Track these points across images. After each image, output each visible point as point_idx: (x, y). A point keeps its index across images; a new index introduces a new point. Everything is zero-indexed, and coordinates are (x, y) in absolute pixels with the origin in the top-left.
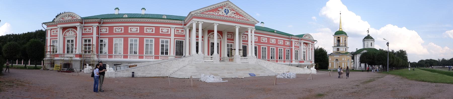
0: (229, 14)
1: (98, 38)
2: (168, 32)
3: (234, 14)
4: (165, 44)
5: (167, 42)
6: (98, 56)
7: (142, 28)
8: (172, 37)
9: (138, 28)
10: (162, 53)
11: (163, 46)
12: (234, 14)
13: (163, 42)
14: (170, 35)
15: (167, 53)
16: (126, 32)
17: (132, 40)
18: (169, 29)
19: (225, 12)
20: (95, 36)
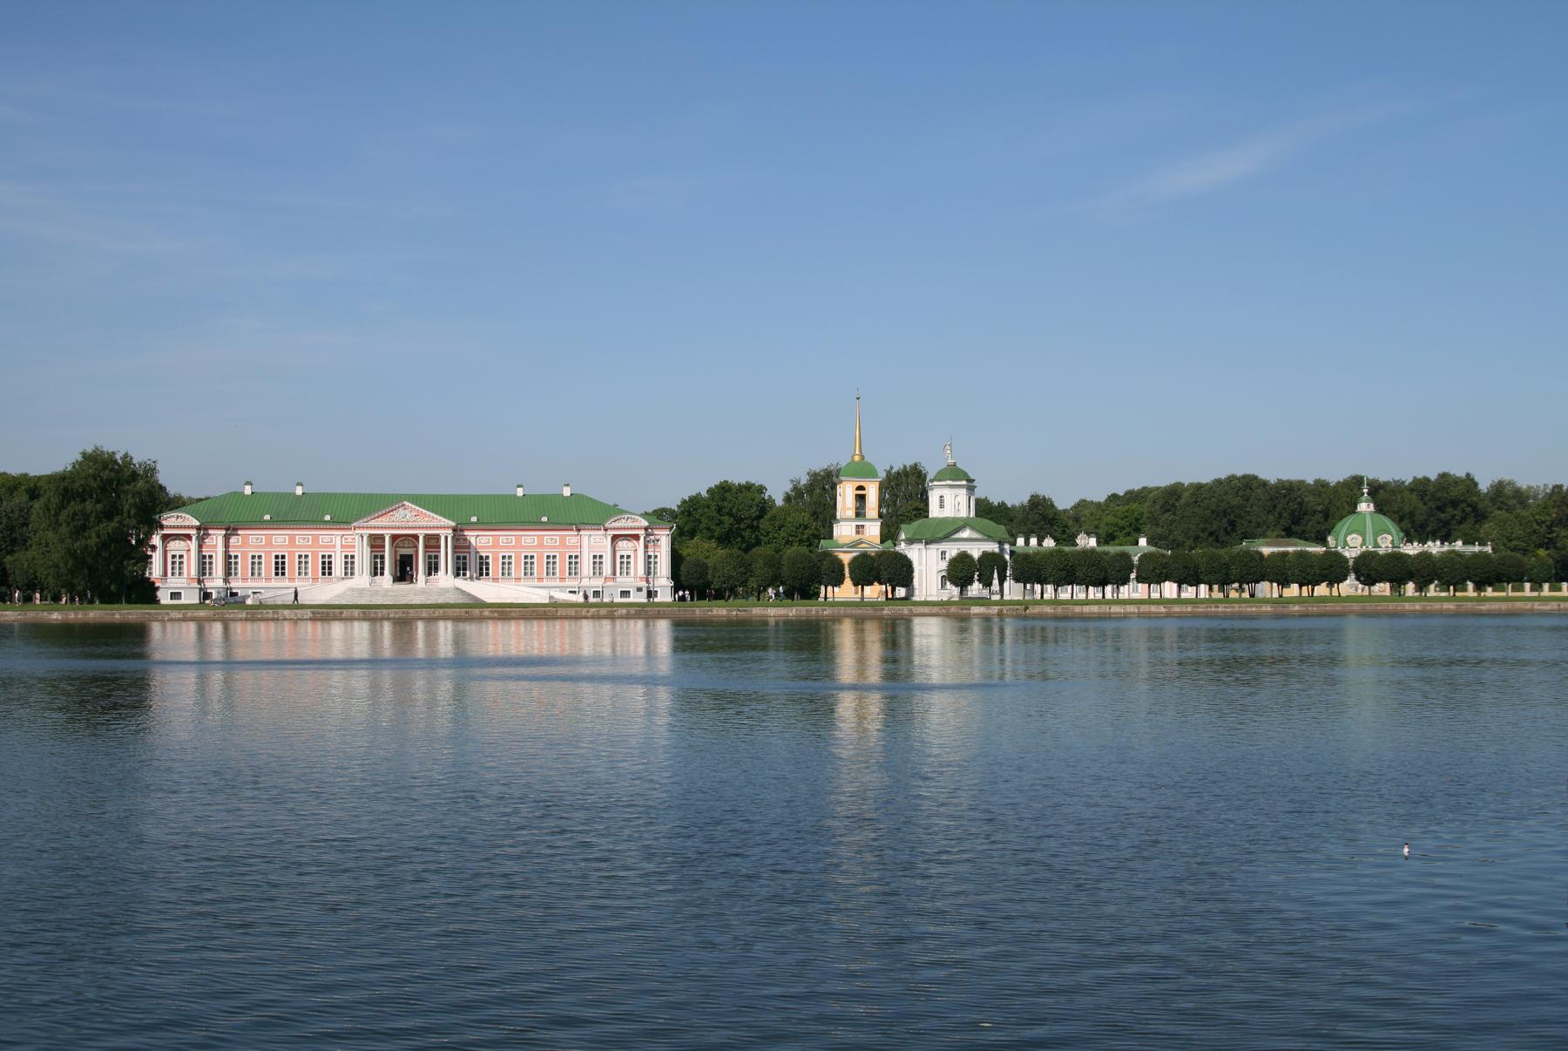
6: (226, 581)
7: (292, 538)
8: (338, 549)
16: (269, 544)
20: (220, 549)
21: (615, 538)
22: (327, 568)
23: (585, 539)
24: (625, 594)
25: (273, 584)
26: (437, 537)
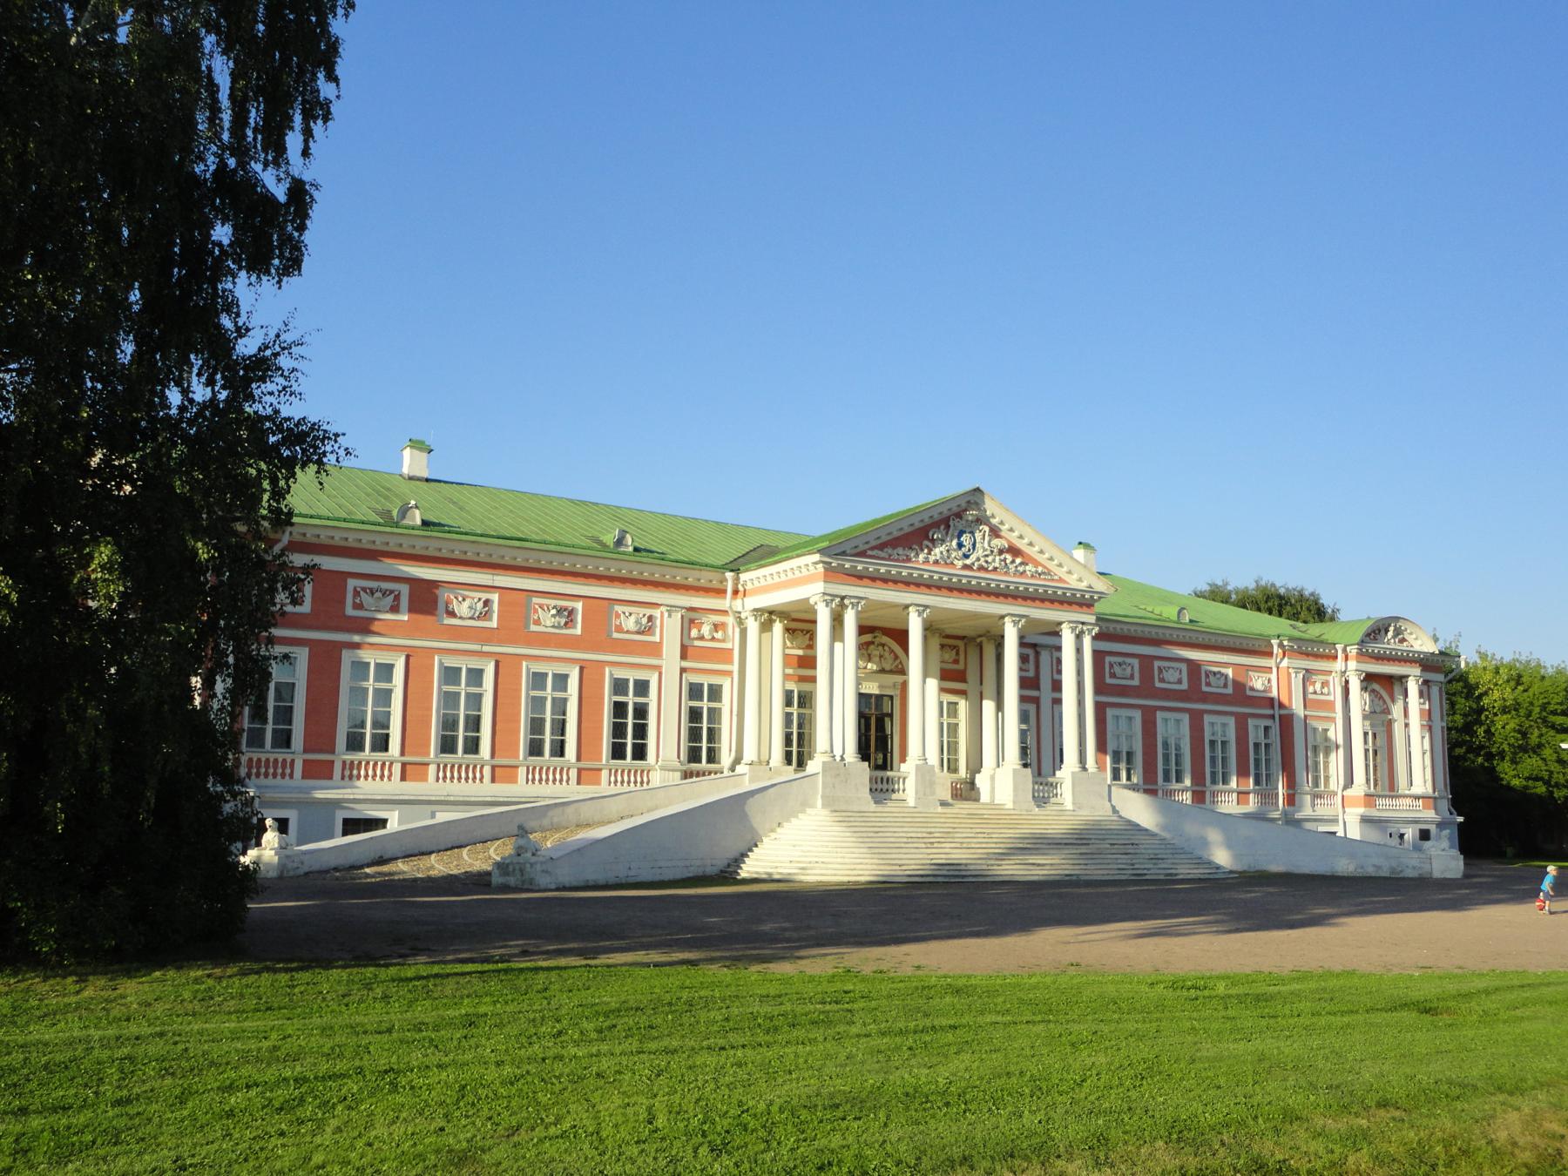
0: (979, 552)
2: (648, 630)
3: (1001, 552)
4: (631, 699)
5: (642, 687)
8: (671, 658)
9: (495, 597)
10: (618, 752)
11: (620, 709)
12: (1001, 552)
13: (620, 686)
14: (655, 649)
15: (640, 753)
17: (451, 675)
18: (657, 613)
19: (960, 545)
22: (630, 737)
25: (430, 787)
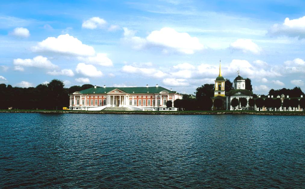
1: (86, 100)
21: (162, 96)
23: (156, 97)
24: (164, 109)
26: (123, 96)
